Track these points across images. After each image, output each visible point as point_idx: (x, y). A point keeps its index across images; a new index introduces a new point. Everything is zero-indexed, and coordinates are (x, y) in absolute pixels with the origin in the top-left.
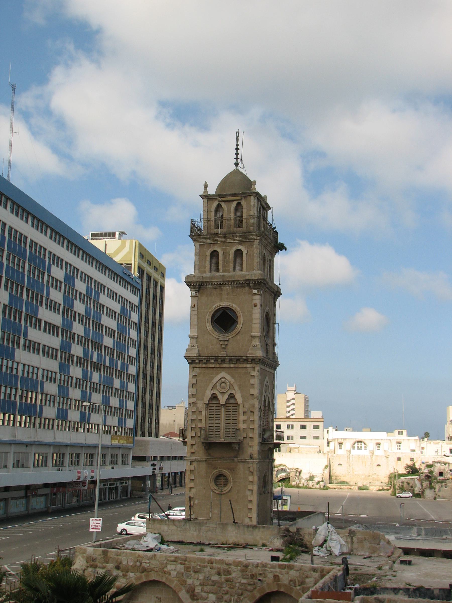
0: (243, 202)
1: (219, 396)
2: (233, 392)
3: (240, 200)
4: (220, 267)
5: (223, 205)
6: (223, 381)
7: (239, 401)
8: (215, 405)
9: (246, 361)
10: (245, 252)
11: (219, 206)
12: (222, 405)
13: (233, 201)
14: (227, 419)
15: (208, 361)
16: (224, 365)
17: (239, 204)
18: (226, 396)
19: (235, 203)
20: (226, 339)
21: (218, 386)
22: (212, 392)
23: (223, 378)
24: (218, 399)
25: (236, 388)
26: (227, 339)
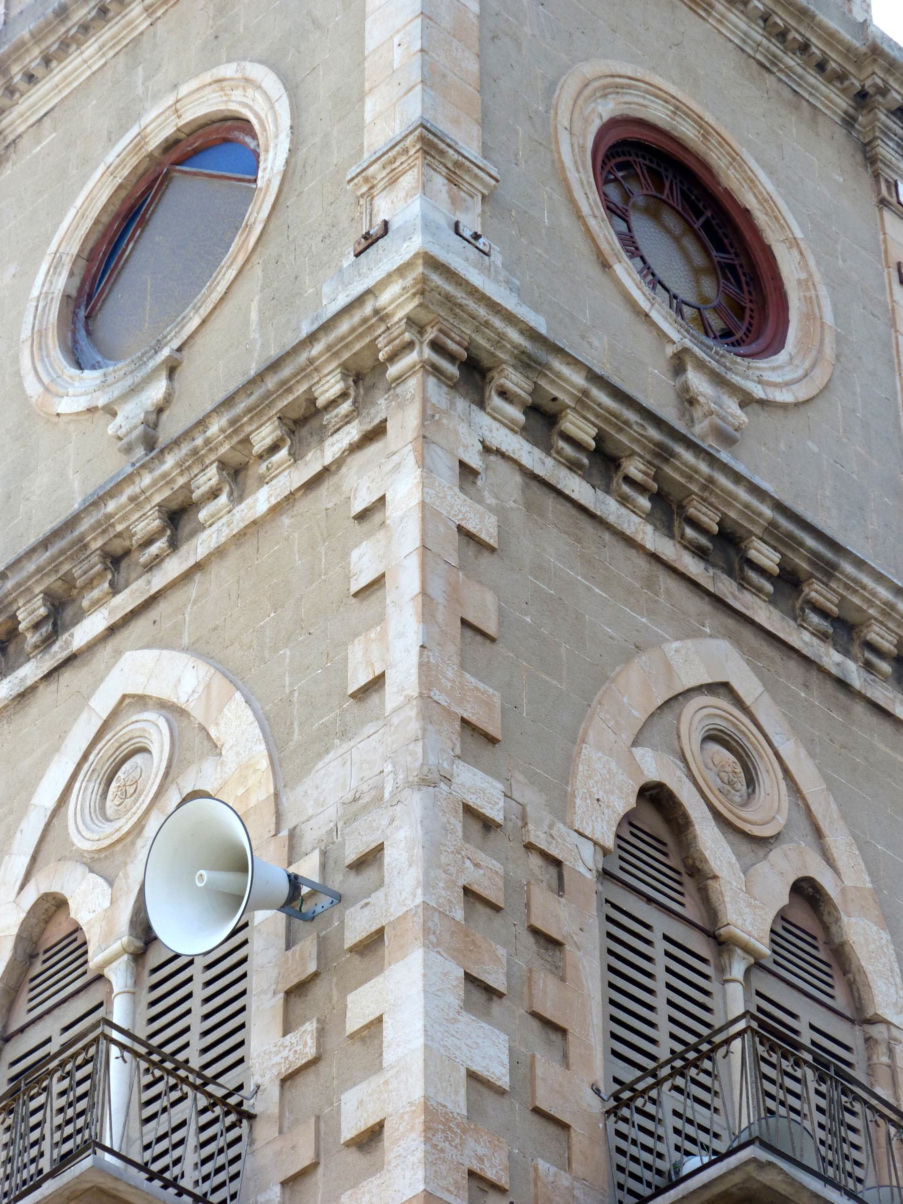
16: (726, 587)
24: (697, 873)
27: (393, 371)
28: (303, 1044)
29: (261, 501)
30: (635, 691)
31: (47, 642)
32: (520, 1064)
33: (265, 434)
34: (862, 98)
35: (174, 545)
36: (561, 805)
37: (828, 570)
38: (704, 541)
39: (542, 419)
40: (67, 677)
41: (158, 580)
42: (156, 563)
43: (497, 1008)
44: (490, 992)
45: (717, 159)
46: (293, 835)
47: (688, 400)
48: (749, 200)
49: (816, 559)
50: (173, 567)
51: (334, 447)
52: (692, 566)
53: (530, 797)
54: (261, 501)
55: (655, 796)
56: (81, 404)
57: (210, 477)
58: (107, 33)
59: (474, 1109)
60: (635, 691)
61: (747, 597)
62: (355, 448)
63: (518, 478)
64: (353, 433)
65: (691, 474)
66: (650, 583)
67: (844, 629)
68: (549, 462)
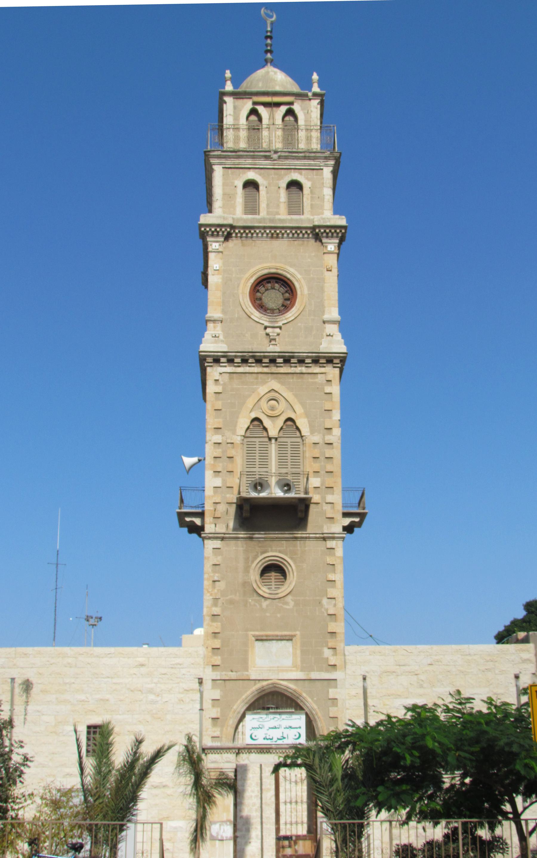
0: (296, 107)
1: (267, 423)
2: (293, 416)
3: (291, 103)
4: (263, 205)
5: (261, 109)
6: (274, 397)
7: (305, 431)
8: (257, 440)
9: (316, 361)
10: (307, 185)
11: (254, 112)
12: (270, 439)
13: (278, 105)
14: (282, 462)
15: (245, 361)
16: (274, 369)
17: (290, 112)
18: (280, 422)
19: (283, 109)
20: (276, 325)
21: (263, 403)
22: (253, 415)
23: (273, 390)
24: (265, 429)
25: (298, 408)
26: (280, 324)
30: (250, 402)
32: (224, 481)
34: (317, 234)
36: (234, 432)
37: (293, 357)
38: (267, 365)
39: (231, 361)
43: (220, 474)
44: (219, 472)
45: (280, 272)
47: (268, 334)
48: (289, 276)
49: (289, 356)
52: (266, 370)
53: (228, 434)
55: (257, 419)
59: (215, 492)
60: (250, 402)
61: (279, 368)
63: (228, 375)
65: (260, 356)
66: (257, 378)
67: (301, 361)
68: (234, 368)
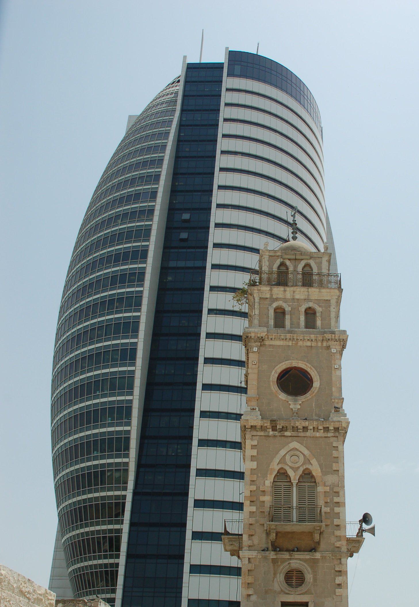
27: (341, 431)
28: (328, 510)
29: (318, 434)
31: (280, 431)
33: (321, 427)
35: (303, 431)
40: (283, 437)
41: (300, 434)
42: (300, 432)
46: (325, 483)
50: (302, 434)
51: (330, 434)
54: (318, 434)
56: (284, 399)
57: (312, 428)
58: (285, 342)
62: (332, 436)
64: (332, 434)
